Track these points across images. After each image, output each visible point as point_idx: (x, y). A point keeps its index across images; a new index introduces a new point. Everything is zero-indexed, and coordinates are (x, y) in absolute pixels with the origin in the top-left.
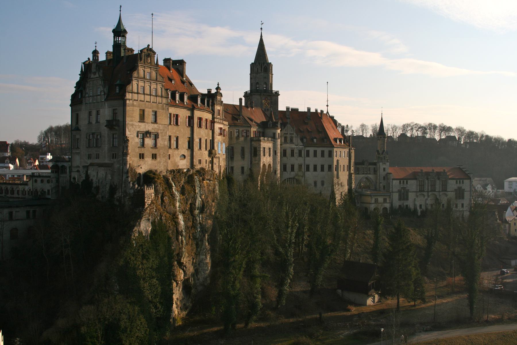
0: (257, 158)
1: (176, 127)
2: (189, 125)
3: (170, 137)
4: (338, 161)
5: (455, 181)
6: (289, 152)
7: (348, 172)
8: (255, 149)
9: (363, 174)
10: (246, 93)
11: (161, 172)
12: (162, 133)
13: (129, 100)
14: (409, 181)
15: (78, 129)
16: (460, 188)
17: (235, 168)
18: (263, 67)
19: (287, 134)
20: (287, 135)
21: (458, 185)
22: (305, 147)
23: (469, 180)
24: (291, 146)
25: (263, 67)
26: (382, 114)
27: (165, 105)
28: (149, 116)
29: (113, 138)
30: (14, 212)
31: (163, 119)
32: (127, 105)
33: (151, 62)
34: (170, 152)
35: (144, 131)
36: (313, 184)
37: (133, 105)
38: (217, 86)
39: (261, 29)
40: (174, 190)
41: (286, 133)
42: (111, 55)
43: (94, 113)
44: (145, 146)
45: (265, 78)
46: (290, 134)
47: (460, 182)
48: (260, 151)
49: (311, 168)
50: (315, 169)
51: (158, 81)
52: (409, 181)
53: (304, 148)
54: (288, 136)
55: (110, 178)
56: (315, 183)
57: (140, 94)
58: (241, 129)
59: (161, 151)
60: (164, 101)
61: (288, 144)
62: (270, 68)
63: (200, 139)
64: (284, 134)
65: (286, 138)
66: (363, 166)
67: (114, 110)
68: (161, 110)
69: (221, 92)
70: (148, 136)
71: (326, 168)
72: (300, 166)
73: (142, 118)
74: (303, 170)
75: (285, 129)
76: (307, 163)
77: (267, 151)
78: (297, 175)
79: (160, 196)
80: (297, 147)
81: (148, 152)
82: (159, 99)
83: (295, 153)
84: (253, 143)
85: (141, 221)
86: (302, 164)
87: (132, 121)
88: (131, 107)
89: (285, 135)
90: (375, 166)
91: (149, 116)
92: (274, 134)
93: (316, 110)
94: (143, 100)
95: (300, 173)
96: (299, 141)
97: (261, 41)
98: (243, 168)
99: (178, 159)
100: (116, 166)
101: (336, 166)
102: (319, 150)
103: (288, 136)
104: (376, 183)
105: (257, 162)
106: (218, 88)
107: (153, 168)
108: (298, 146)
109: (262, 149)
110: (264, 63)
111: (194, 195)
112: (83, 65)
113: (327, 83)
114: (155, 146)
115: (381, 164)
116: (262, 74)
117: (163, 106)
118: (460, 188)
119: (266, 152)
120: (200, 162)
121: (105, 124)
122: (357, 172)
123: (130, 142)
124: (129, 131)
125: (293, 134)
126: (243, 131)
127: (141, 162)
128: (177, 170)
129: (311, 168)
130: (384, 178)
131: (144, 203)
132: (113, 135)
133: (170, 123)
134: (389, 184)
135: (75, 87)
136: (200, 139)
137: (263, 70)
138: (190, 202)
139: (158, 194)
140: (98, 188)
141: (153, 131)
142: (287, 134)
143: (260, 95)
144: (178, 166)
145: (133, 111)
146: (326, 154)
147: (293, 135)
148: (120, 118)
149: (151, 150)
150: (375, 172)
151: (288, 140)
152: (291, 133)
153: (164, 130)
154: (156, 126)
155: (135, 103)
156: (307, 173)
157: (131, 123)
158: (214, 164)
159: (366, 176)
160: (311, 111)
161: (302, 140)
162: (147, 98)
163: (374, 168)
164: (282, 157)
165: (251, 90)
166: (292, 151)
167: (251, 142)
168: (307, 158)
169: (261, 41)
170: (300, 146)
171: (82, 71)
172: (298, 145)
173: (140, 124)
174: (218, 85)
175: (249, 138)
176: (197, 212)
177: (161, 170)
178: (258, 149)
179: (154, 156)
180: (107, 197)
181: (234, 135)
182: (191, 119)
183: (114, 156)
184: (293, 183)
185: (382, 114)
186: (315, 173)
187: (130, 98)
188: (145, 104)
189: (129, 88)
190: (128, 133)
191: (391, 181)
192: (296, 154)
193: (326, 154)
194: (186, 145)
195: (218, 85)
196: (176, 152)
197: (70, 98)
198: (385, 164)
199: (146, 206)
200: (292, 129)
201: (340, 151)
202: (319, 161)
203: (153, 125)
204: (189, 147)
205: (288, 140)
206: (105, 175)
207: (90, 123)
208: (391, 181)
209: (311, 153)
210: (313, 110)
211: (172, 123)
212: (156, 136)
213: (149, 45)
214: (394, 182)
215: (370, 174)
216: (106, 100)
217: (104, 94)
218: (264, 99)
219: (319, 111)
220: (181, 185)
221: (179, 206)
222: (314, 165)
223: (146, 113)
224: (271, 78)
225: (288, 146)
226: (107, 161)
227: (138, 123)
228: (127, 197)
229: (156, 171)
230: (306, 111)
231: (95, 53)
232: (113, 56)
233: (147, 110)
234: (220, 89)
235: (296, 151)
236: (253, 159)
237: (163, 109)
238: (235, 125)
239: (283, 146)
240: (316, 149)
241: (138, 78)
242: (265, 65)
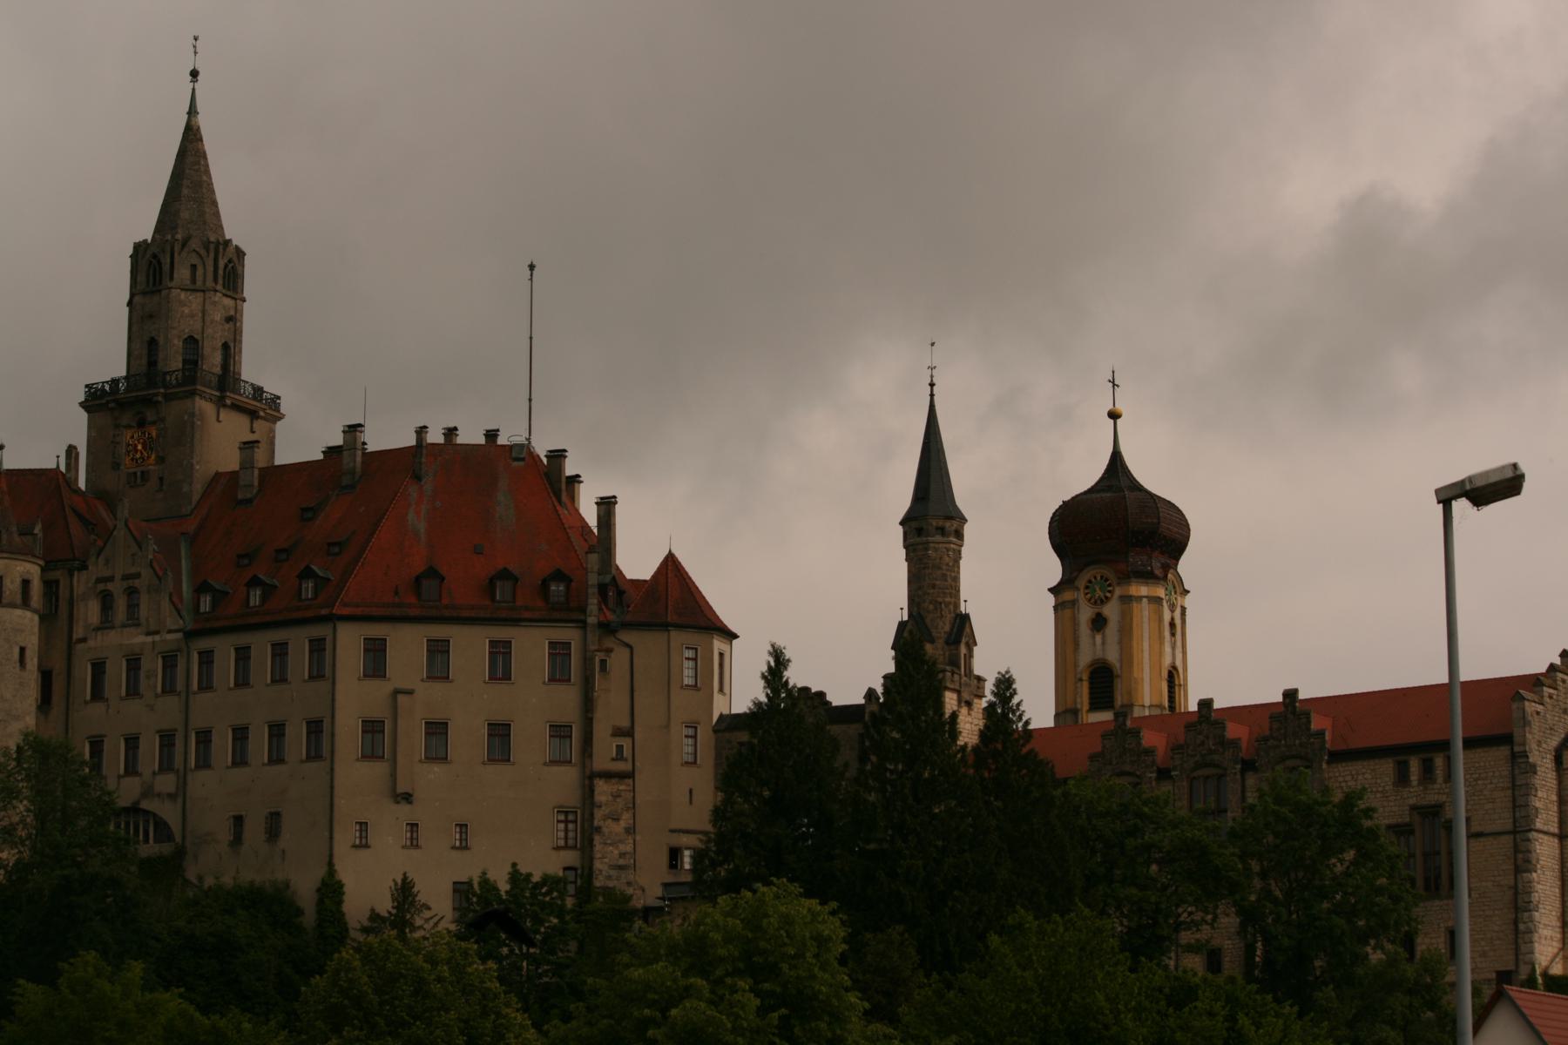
5: (1387, 767)
6: (117, 674)
19: (111, 579)
20: (110, 586)
21: (1415, 794)
22: (190, 635)
23: (1504, 751)
24: (127, 642)
25: (221, 264)
26: (932, 385)
39: (194, 74)
41: (107, 573)
45: (151, 316)
46: (126, 577)
49: (223, 744)
54: (116, 588)
61: (113, 633)
64: (99, 580)
71: (296, 737)
72: (167, 739)
75: (101, 560)
78: (148, 792)
80: (153, 642)
83: (142, 674)
86: (176, 730)
89: (101, 587)
95: (167, 783)
97: (192, 135)
102: (261, 644)
103: (116, 588)
108: (157, 638)
113: (532, 267)
125: (138, 576)
129: (223, 744)
142: (111, 579)
147: (137, 581)
151: (121, 604)
152: (133, 570)
160: (378, 439)
164: (86, 703)
166: (134, 664)
169: (192, 135)
170: (170, 637)
172: (157, 633)
184: (141, 837)
185: (932, 385)
192: (148, 677)
193: (299, 659)
205: (121, 604)
218: (128, 427)
235: (153, 665)
239: (91, 643)
240: (243, 639)
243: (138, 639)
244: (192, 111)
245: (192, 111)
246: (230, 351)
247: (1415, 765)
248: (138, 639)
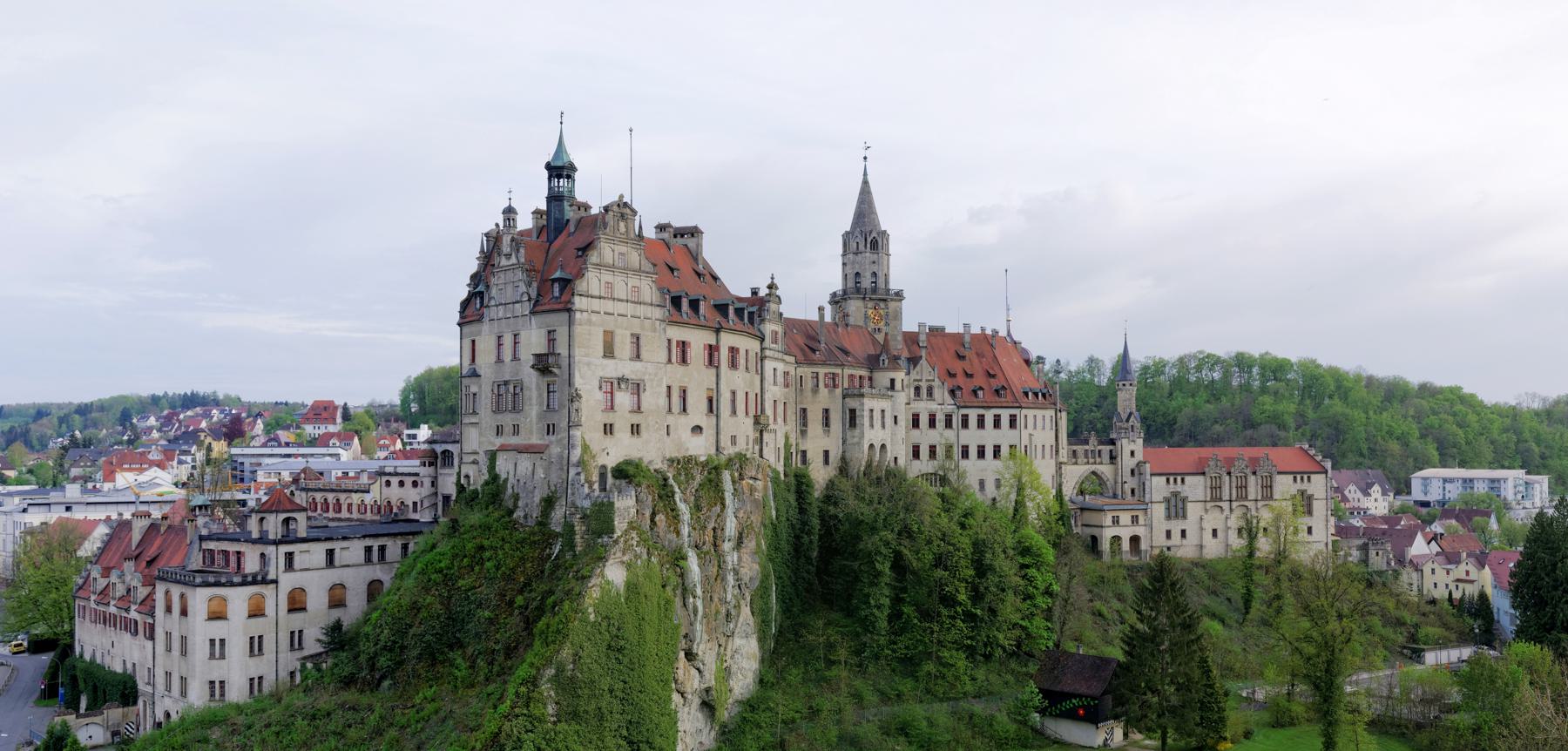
0: (857, 432)
1: (681, 369)
2: (711, 362)
3: (669, 387)
4: (1031, 435)
7: (1053, 462)
8: (853, 412)
9: (1088, 463)
10: (834, 295)
11: (650, 462)
12: (652, 380)
13: (582, 311)
14: (1187, 479)
15: (474, 374)
16: (1176, 494)
17: (809, 455)
18: (869, 240)
19: (921, 380)
22: (958, 408)
25: (869, 240)
27: (658, 322)
28: (624, 347)
29: (548, 392)
30: (337, 552)
31: (655, 351)
32: (577, 321)
33: (627, 232)
34: (671, 420)
35: (615, 375)
36: (977, 487)
37: (589, 322)
38: (769, 281)
39: (865, 158)
40: (677, 499)
41: (919, 378)
42: (544, 217)
43: (508, 341)
44: (616, 408)
47: (1175, 480)
48: (863, 416)
49: (973, 452)
50: (981, 453)
51: (644, 272)
52: (1187, 479)
53: (956, 411)
54: (924, 385)
55: (542, 476)
56: (982, 483)
57: (604, 298)
58: (822, 371)
59: (650, 418)
60: (658, 313)
62: (885, 242)
63: (734, 393)
64: (915, 380)
65: (917, 389)
66: (1087, 447)
67: (549, 332)
68: (649, 333)
69: (778, 293)
70: (623, 386)
72: (949, 449)
73: (609, 352)
74: (956, 458)
76: (963, 442)
77: (877, 415)
78: (942, 467)
79: (648, 514)
81: (622, 421)
82: (641, 310)
84: (847, 400)
85: (604, 566)
87: (587, 355)
88: (588, 327)
90: (1111, 447)
91: (624, 347)
92: (893, 381)
93: (983, 329)
94: (612, 312)
96: (946, 394)
98: (826, 453)
99: (685, 434)
100: (555, 450)
101: (1026, 447)
103: (924, 385)
104: (1116, 482)
105: (856, 440)
106: (770, 287)
107: (634, 455)
109: (866, 413)
110: (871, 232)
111: (722, 511)
112: (485, 238)
114: (638, 409)
115: (1125, 441)
116: (868, 254)
117: (653, 324)
118: (1176, 494)
119: (875, 418)
120: (734, 440)
121: (532, 363)
122: (1074, 460)
123: (584, 399)
124: (581, 377)
126: (826, 375)
127: (608, 441)
128: (684, 457)
129: (973, 452)
130: (1132, 472)
131: (610, 530)
132: (548, 385)
133: (670, 361)
134: (1144, 484)
135: (469, 285)
136: (734, 393)
137: (868, 245)
138: (712, 525)
139: (644, 509)
140: (516, 497)
141: (633, 377)
142: (921, 380)
143: (864, 298)
144: (688, 449)
145: (590, 334)
146: (1005, 422)
148: (562, 349)
149: (629, 415)
150: (1113, 458)
151: (924, 392)
153: (656, 375)
154: (638, 365)
155: (594, 317)
156: (964, 463)
157: (586, 359)
158: (764, 444)
159: (1093, 468)
161: (952, 393)
162: (621, 308)
163: (1111, 451)
165: (845, 292)
167: (844, 398)
168: (963, 433)
171: (482, 251)
173: (606, 361)
174: (772, 278)
175: (839, 391)
176: (727, 546)
177: (650, 459)
178: (858, 413)
179: (635, 429)
180: (534, 516)
181: (806, 383)
182: (712, 350)
183: (550, 429)
186: (981, 462)
187: (584, 307)
188: (616, 321)
189: (581, 286)
190: (578, 382)
191: (1148, 477)
193: (1005, 422)
194: (704, 405)
195: (772, 278)
196: (683, 419)
197: (458, 308)
198: (1133, 441)
199: (618, 533)
200: (930, 369)
201: (883, 411)
202: (989, 437)
203: (633, 363)
204: (711, 410)
205: (924, 392)
206: (530, 469)
207: (499, 360)
208: (1148, 477)
209: (973, 421)
210: (975, 330)
211: (674, 359)
212: (638, 388)
213: (621, 196)
214: (1155, 479)
215: (1101, 463)
216: (533, 313)
217: (529, 300)
219: (989, 332)
220: (693, 490)
221: (689, 533)
222: (930, 447)
223: (617, 340)
224: (885, 263)
225: (924, 407)
226: (535, 440)
227: (602, 360)
228: (578, 516)
229: (640, 459)
230: (962, 331)
231: (509, 212)
232: (548, 220)
233: (618, 332)
234: (777, 288)
235: (940, 418)
236: (849, 434)
237: (654, 330)
238: (811, 363)
239: (912, 405)
241: (599, 266)
242: (874, 234)
243: (933, 406)
244: (865, 174)
245: (865, 174)
246: (887, 276)
247: (1305, 477)
248: (933, 406)
